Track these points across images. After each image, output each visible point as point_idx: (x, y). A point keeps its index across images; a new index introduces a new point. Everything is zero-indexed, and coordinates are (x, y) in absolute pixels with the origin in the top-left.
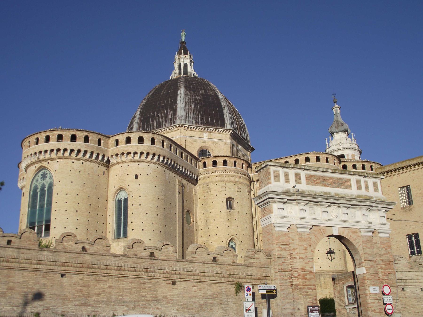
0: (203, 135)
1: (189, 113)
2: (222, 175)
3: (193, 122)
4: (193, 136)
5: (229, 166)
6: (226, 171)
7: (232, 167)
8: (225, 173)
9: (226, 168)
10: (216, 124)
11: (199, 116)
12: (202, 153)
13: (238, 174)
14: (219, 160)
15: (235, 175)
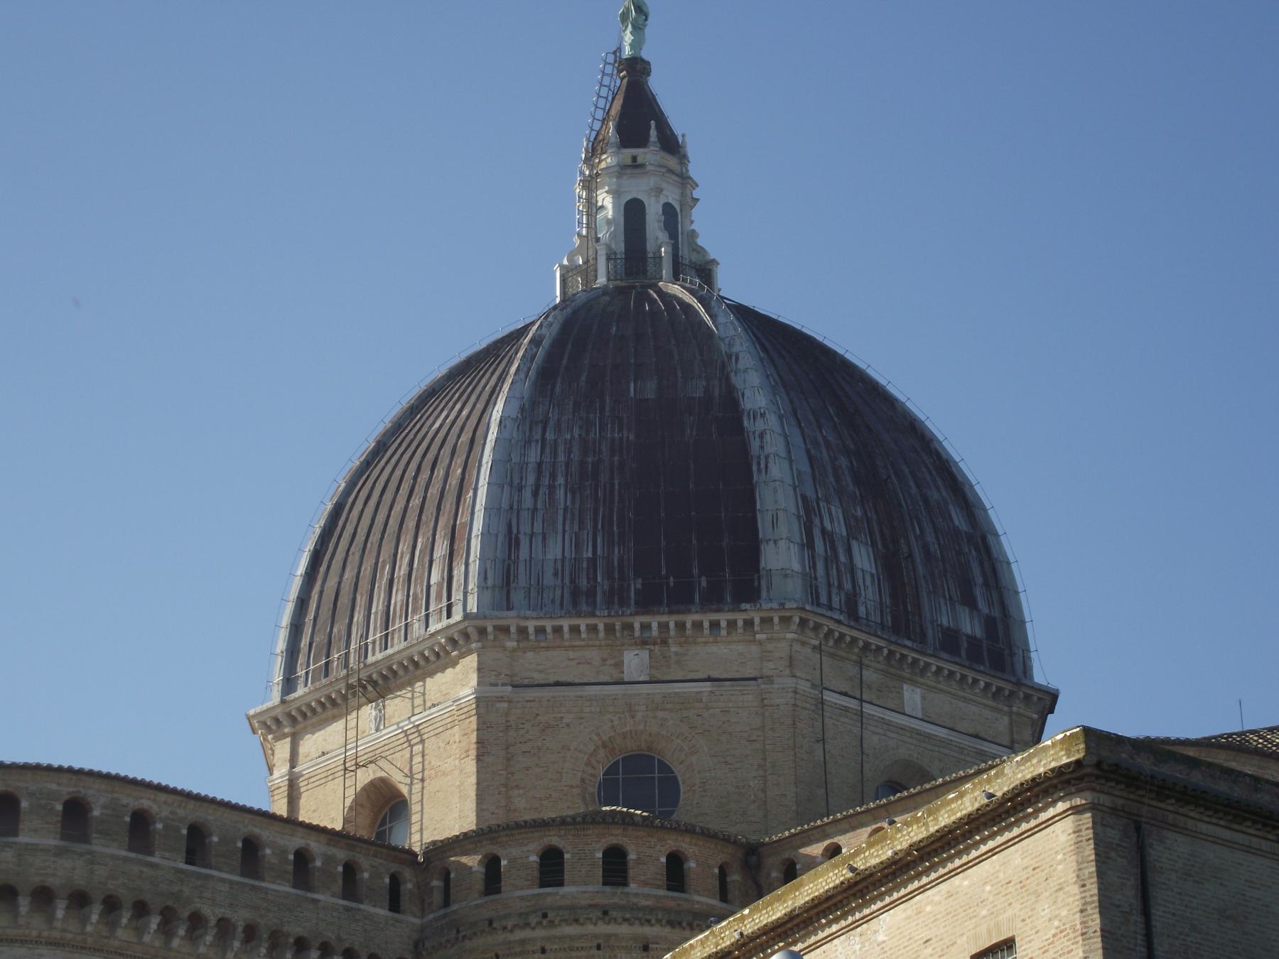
0: (619, 665)
1: (538, 541)
2: (523, 942)
3: (558, 592)
4: (552, 679)
5: (574, 883)
6: (545, 916)
7: (590, 888)
8: (540, 933)
9: (549, 900)
10: (704, 584)
11: (599, 552)
12: (656, 775)
13: (624, 929)
14: (515, 851)
15: (608, 936)
